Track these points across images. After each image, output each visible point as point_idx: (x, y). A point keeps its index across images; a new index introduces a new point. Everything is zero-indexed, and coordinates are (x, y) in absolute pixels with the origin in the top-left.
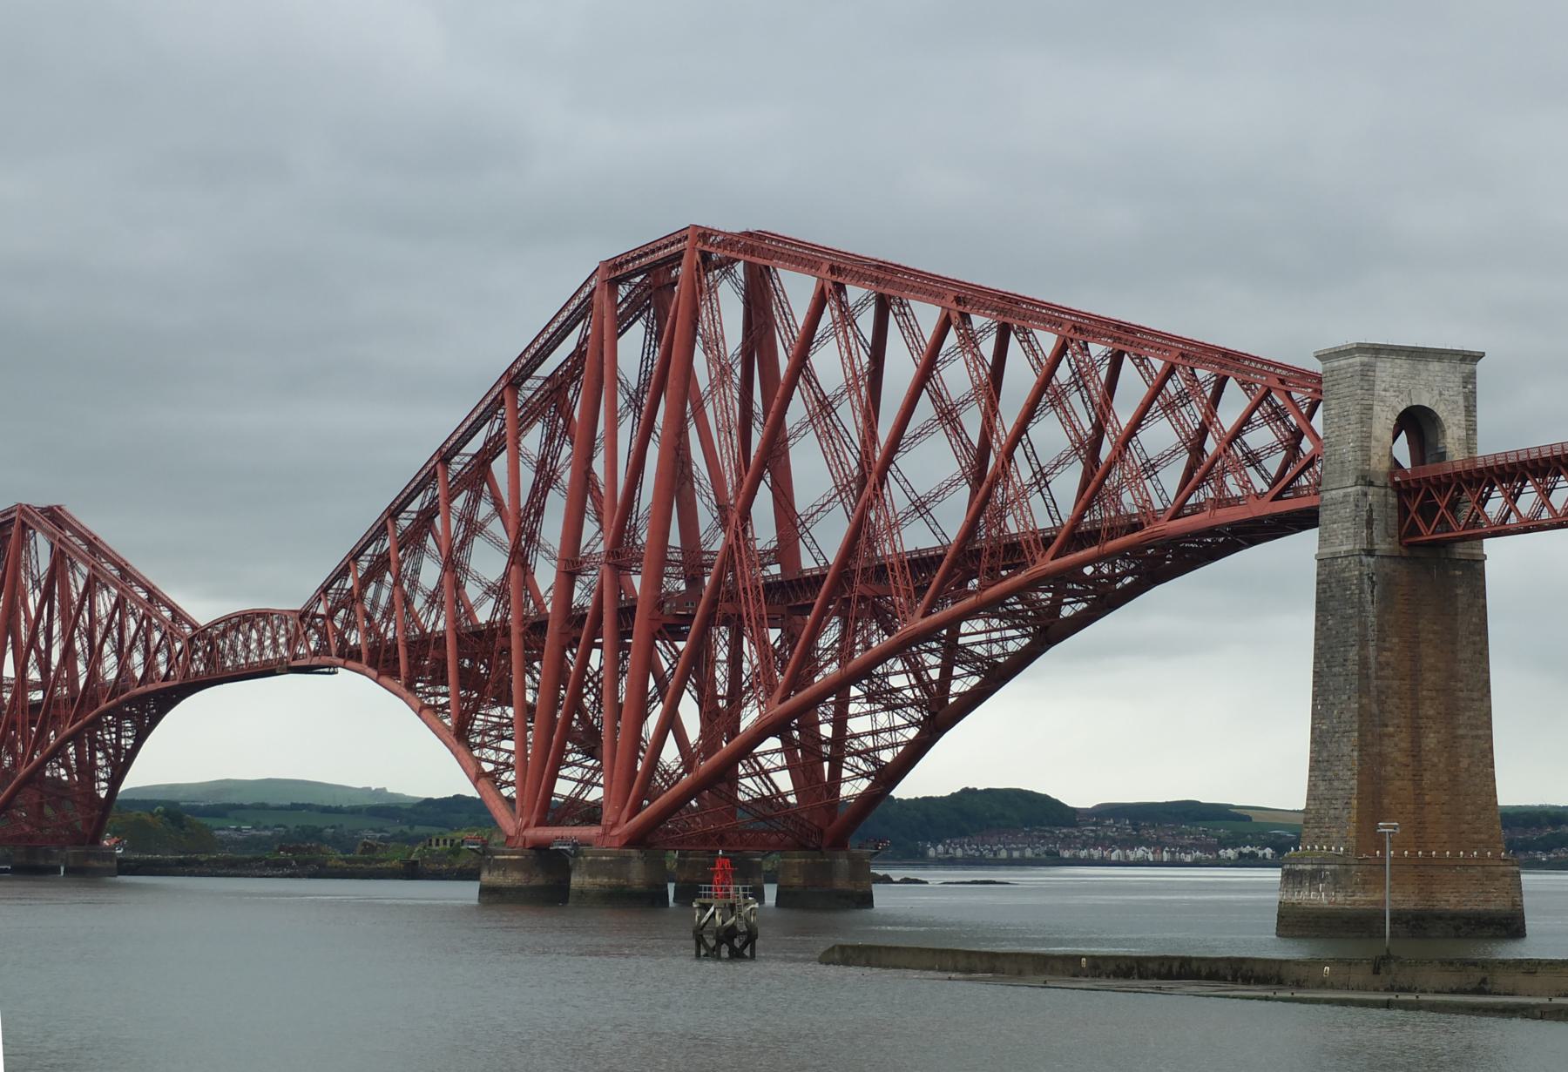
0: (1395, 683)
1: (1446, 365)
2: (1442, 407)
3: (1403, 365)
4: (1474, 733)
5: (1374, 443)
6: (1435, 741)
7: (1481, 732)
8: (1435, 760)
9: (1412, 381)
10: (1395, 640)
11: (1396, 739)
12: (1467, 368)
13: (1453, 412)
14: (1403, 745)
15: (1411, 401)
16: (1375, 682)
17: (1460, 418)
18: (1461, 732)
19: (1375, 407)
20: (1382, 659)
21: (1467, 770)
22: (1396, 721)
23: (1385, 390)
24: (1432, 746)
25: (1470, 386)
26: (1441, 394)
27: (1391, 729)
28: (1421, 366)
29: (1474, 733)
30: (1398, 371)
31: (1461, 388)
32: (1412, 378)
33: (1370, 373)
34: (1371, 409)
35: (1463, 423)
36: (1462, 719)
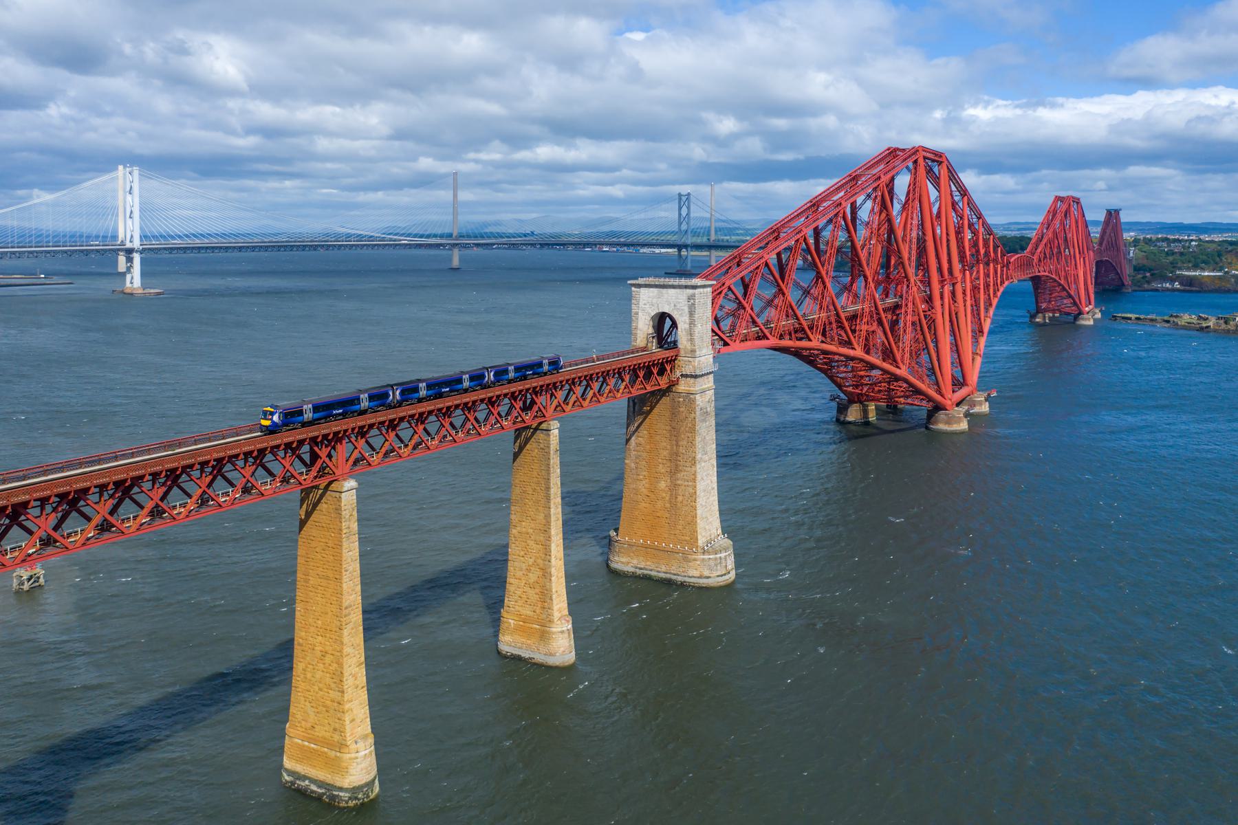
0: (645, 454)
1: (678, 290)
2: (676, 313)
3: (655, 290)
4: (686, 483)
5: (638, 332)
6: (665, 485)
7: (690, 483)
8: (664, 495)
9: (660, 299)
10: (645, 432)
11: (644, 482)
12: (690, 291)
13: (681, 315)
14: (647, 485)
15: (658, 309)
16: (634, 453)
17: (686, 318)
18: (679, 482)
19: (640, 314)
20: (638, 441)
21: (682, 502)
22: (644, 473)
23: (645, 304)
24: (662, 487)
25: (692, 301)
26: (675, 306)
27: (641, 477)
28: (664, 291)
29: (686, 483)
30: (651, 294)
31: (686, 303)
32: (659, 298)
33: (637, 296)
34: (638, 314)
35: (688, 321)
36: (679, 475)
